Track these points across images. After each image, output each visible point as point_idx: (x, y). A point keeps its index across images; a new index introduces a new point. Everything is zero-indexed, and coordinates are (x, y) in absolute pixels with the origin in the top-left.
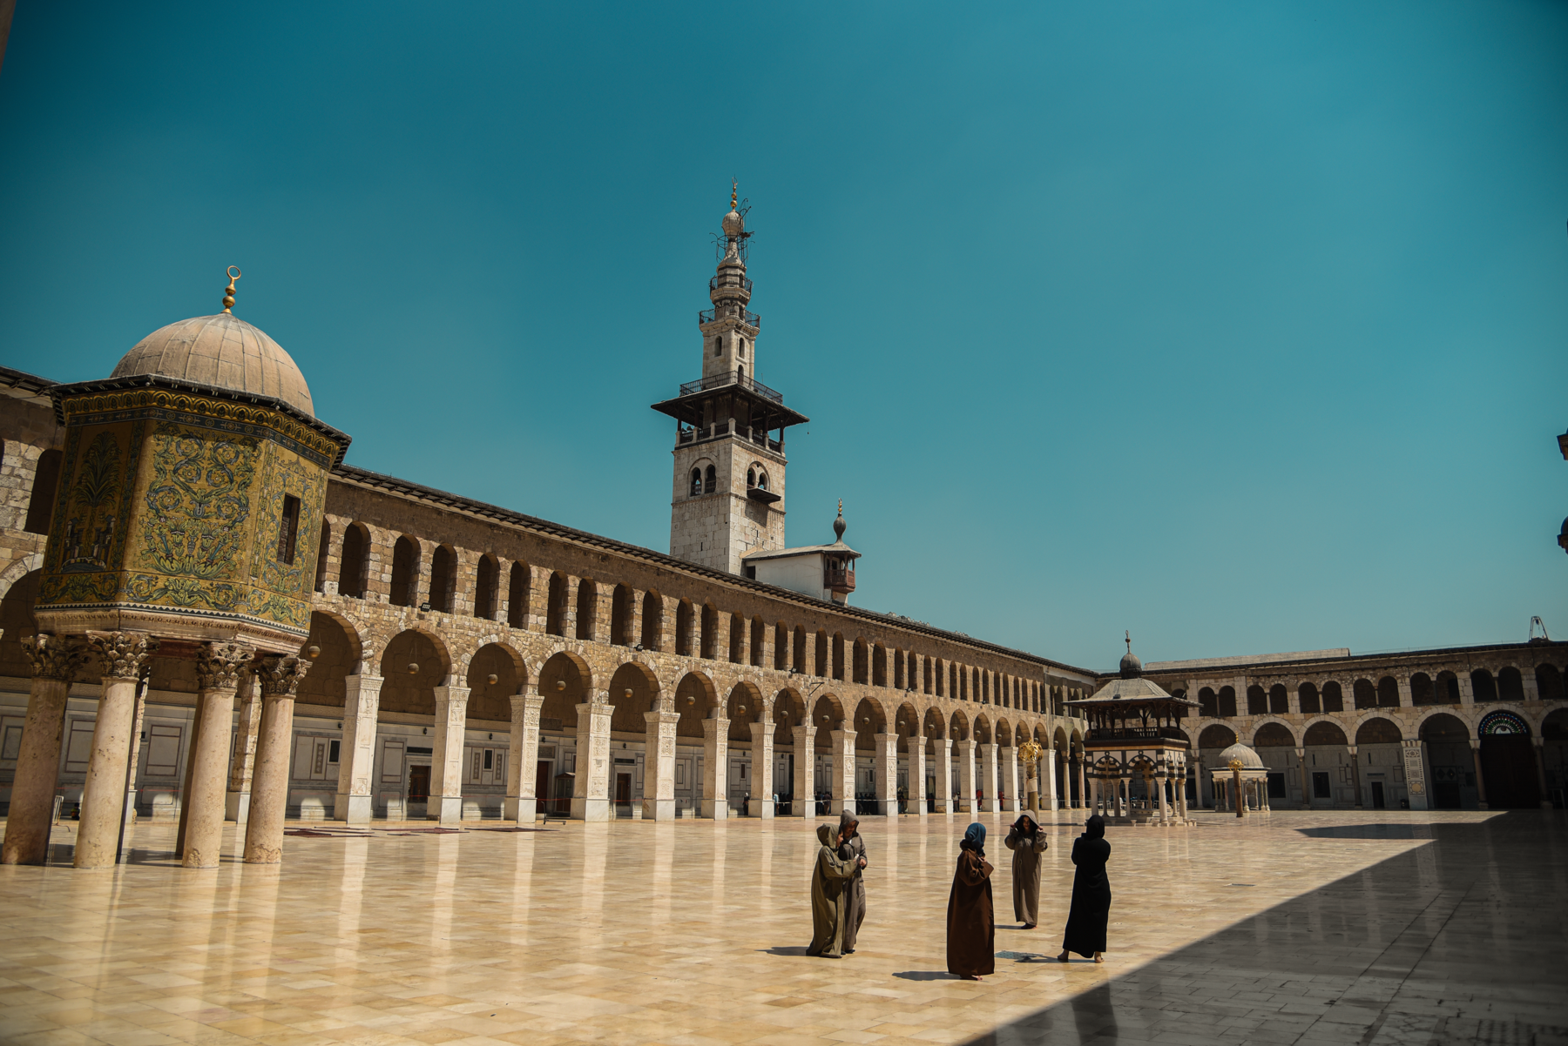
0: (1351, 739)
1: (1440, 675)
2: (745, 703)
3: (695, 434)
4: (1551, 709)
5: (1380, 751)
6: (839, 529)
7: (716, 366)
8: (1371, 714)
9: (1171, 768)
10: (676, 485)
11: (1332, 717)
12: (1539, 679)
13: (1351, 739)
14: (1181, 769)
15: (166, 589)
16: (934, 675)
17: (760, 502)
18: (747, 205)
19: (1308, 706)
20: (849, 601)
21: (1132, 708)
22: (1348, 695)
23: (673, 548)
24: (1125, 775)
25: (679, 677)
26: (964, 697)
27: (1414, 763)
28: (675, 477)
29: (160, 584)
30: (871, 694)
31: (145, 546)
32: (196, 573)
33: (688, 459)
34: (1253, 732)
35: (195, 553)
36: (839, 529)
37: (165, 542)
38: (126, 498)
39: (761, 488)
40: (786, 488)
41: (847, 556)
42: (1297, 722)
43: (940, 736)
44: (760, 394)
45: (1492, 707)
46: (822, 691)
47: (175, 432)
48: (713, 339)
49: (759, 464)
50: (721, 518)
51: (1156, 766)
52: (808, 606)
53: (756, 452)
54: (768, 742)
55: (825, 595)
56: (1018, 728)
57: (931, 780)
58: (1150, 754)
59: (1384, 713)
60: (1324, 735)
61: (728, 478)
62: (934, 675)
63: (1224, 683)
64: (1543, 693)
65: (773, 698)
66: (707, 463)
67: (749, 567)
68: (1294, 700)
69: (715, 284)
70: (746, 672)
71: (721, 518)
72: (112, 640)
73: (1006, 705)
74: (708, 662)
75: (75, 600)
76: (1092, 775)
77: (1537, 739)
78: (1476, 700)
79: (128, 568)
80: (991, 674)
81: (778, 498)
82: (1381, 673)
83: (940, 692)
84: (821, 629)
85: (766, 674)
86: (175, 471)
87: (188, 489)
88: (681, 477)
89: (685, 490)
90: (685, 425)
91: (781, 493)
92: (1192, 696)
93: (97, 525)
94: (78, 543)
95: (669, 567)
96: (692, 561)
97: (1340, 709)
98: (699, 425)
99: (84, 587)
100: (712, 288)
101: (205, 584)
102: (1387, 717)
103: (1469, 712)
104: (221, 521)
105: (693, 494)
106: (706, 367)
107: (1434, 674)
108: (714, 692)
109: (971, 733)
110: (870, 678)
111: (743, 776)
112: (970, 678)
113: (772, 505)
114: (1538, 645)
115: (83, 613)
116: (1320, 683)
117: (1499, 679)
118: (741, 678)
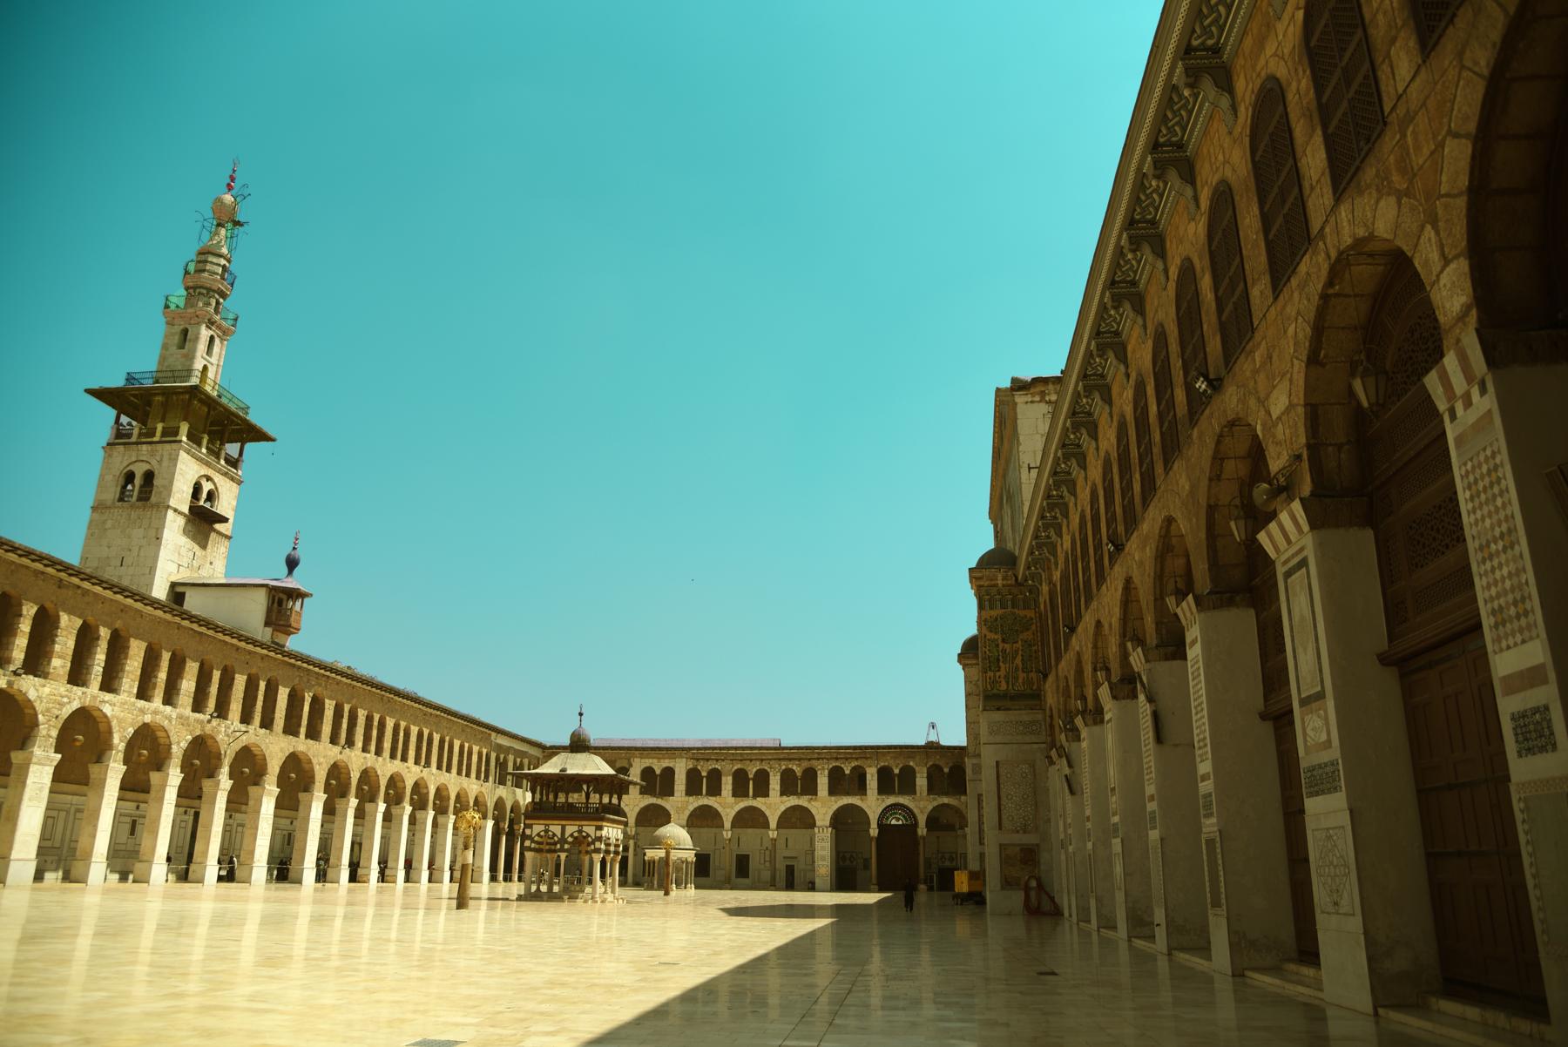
0: (773, 824)
1: (854, 769)
2: (147, 749)
3: (136, 432)
4: (935, 804)
5: (797, 835)
6: (292, 564)
7: (176, 361)
8: (793, 801)
9: (608, 845)
11: (759, 803)
12: (929, 778)
13: (773, 824)
14: (617, 846)
16: (375, 733)
17: (203, 520)
18: (246, 192)
19: (739, 791)
20: (292, 643)
21: (575, 782)
22: (775, 783)
23: (84, 559)
24: (562, 850)
25: (67, 711)
27: (823, 848)
28: (102, 477)
33: (123, 459)
34: (687, 813)
36: (292, 564)
39: (207, 505)
40: (236, 510)
42: (728, 805)
43: (373, 799)
44: (224, 401)
45: (891, 800)
46: (244, 740)
48: (178, 329)
49: (209, 479)
50: (152, 533)
51: (593, 842)
52: (242, 644)
53: (207, 464)
54: (171, 795)
55: (264, 634)
56: (458, 796)
57: (357, 845)
58: (589, 829)
59: (803, 801)
60: (750, 819)
62: (375, 733)
63: (666, 763)
64: (931, 790)
65: (184, 745)
66: (145, 467)
67: (177, 593)
68: (727, 784)
69: (192, 268)
70: (155, 712)
71: (152, 533)
73: (449, 770)
74: (108, 696)
76: (530, 849)
80: (436, 737)
81: (224, 520)
82: (805, 764)
83: (378, 752)
84: (254, 671)
85: (180, 717)
88: (109, 478)
89: (112, 493)
90: (124, 419)
91: (229, 514)
92: (635, 775)
95: (75, 580)
96: (106, 576)
97: (766, 795)
98: (143, 422)
100: (187, 273)
102: (805, 804)
103: (872, 804)
105: (121, 499)
106: (163, 359)
107: (847, 768)
108: (110, 732)
109: (407, 798)
110: (303, 730)
111: (132, 832)
112: (413, 739)
113: (217, 526)
114: (932, 748)
116: (752, 770)
117: (899, 775)
118: (148, 719)
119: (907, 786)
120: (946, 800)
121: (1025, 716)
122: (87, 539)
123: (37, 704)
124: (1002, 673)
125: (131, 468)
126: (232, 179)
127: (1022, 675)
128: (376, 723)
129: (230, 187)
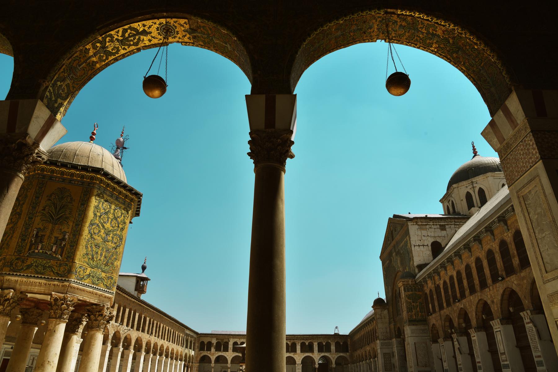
4: (338, 356)
6: (144, 268)
15: (89, 276)
18: (127, 137)
20: (143, 297)
26: (164, 339)
29: (88, 273)
30: (140, 336)
31: (85, 251)
32: (101, 269)
35: (102, 259)
36: (144, 268)
37: (92, 251)
38: (77, 225)
41: (146, 279)
45: (323, 354)
47: (103, 198)
55: (135, 294)
59: (291, 355)
64: (337, 351)
65: (112, 335)
72: (64, 299)
75: (37, 273)
77: (334, 365)
78: (319, 352)
79: (76, 261)
80: (172, 330)
82: (292, 341)
84: (131, 307)
86: (100, 217)
87: (103, 226)
93: (56, 234)
94: (41, 242)
99: (44, 268)
101: (103, 275)
102: (292, 356)
104: (113, 245)
114: (336, 335)
115: (43, 281)
119: (329, 350)
120: (342, 354)
121: (422, 327)
124: (414, 313)
126: (123, 133)
127: (420, 314)
129: (122, 136)
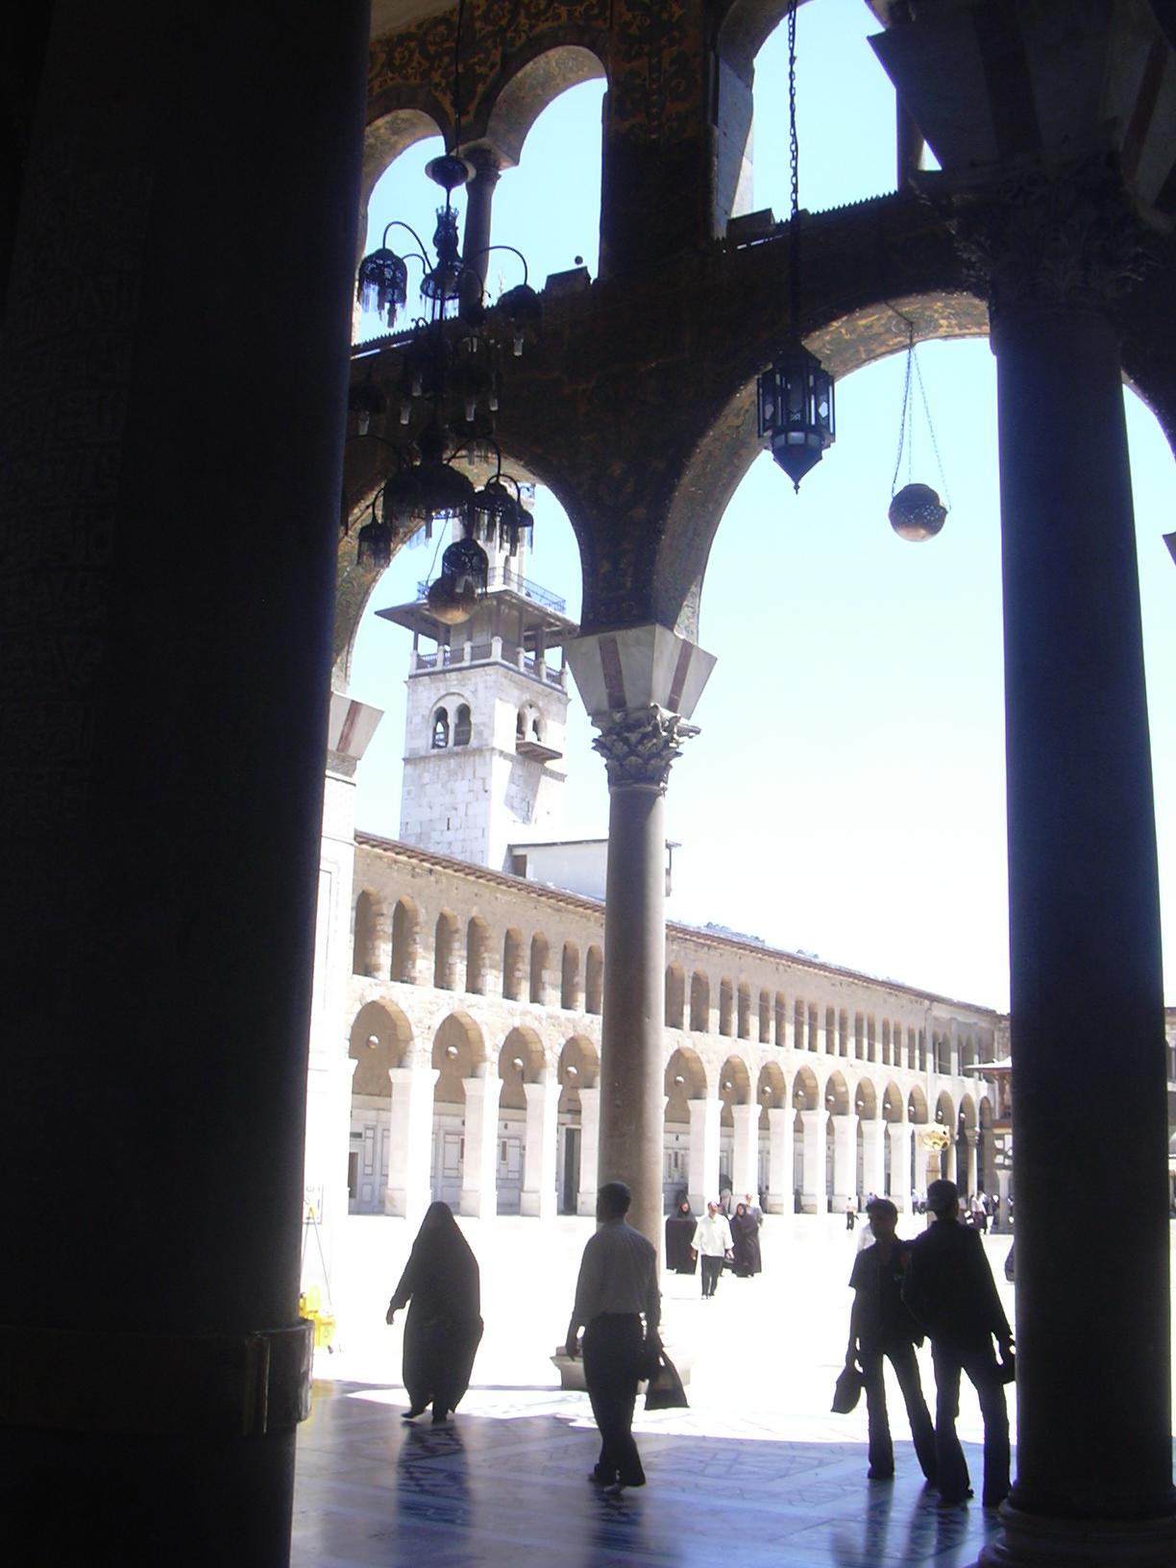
3: (440, 658)
10: (411, 734)
23: (405, 825)
25: (437, 1022)
26: (812, 1048)
28: (409, 720)
33: (430, 695)
50: (478, 785)
56: (887, 1093)
61: (489, 725)
65: (558, 1050)
66: (462, 701)
70: (524, 1013)
88: (418, 719)
89: (424, 742)
96: (432, 849)
105: (435, 746)
108: (482, 1042)
122: (404, 799)
123: (409, 1015)
125: (441, 704)
128: (772, 1003)
